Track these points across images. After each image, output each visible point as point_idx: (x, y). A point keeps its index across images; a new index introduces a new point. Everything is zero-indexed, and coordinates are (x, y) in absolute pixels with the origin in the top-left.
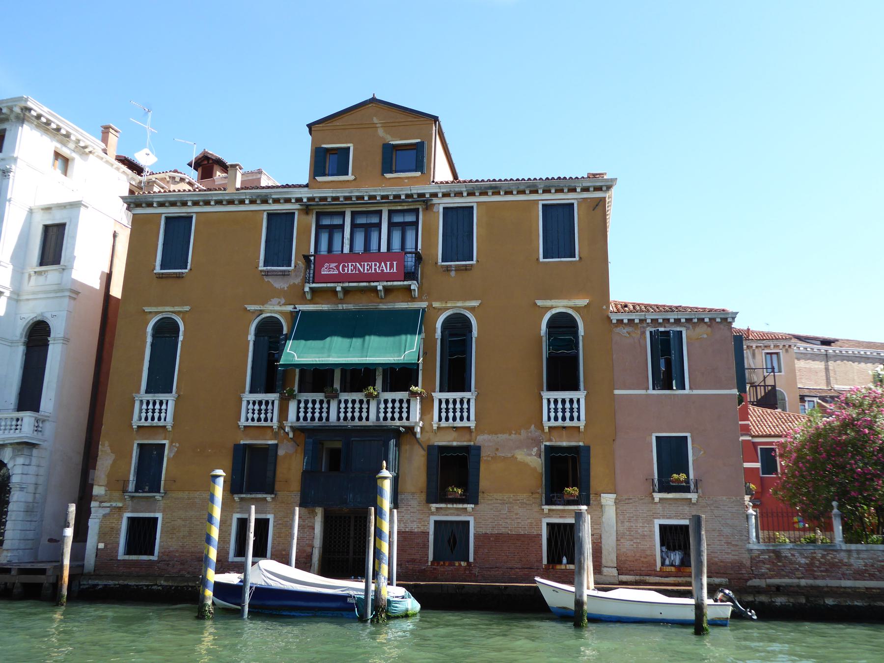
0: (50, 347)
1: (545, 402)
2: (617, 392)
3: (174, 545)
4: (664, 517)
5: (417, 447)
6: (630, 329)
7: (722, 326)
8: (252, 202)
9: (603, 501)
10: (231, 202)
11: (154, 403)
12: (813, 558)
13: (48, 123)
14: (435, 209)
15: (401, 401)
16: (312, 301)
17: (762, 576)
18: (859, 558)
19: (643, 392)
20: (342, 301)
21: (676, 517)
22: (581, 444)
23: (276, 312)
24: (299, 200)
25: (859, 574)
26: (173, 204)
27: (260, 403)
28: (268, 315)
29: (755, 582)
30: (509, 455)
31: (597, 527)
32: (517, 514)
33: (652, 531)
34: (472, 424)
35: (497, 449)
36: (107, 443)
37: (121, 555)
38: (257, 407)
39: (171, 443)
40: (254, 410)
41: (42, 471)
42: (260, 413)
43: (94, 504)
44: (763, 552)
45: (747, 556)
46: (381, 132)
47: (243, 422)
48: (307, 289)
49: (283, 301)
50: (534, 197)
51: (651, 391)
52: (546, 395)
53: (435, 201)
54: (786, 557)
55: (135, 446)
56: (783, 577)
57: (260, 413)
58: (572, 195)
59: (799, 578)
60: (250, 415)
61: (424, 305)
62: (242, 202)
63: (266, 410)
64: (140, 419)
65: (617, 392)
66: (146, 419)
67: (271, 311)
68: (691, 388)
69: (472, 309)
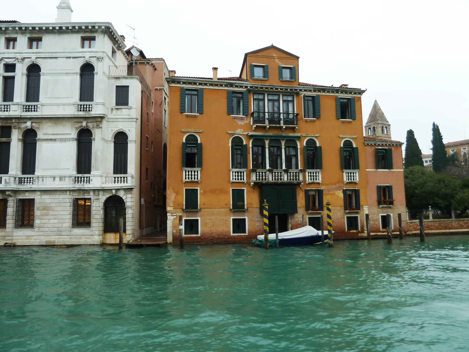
0: (129, 144)
2: (367, 170)
3: (207, 230)
5: (300, 190)
8: (226, 86)
9: (364, 209)
10: (216, 85)
11: (192, 172)
15: (296, 173)
16: (254, 131)
17: (411, 231)
20: (267, 131)
24: (246, 87)
26: (190, 83)
27: (238, 173)
33: (379, 218)
36: (171, 189)
37: (184, 235)
38: (237, 174)
42: (238, 177)
43: (168, 214)
46: (277, 61)
49: (242, 130)
52: (345, 171)
53: (301, 93)
57: (238, 177)
60: (234, 177)
61: (299, 135)
62: (221, 85)
63: (241, 175)
64: (186, 178)
65: (367, 170)
66: (189, 178)
67: (238, 134)
69: (317, 137)
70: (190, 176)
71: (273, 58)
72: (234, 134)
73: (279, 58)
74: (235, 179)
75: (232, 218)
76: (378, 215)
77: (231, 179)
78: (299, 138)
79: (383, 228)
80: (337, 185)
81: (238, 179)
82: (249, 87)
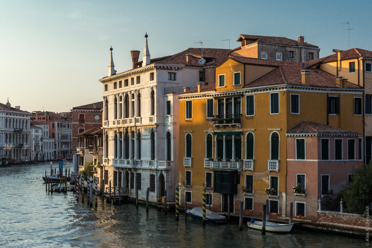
2: (288, 160)
6: (291, 138)
7: (315, 137)
12: (334, 216)
13: (164, 67)
14: (244, 97)
18: (346, 217)
19: (293, 160)
23: (210, 132)
24: (213, 95)
25: (346, 222)
28: (209, 133)
29: (318, 222)
30: (262, 179)
31: (281, 202)
34: (252, 169)
36: (180, 171)
39: (192, 171)
41: (172, 177)
44: (321, 213)
45: (317, 214)
47: (205, 166)
48: (214, 126)
50: (268, 91)
51: (296, 160)
54: (327, 215)
56: (325, 221)
58: (277, 91)
59: (329, 222)
65: (288, 160)
67: (210, 132)
68: (306, 159)
72: (208, 132)
79: (298, 215)
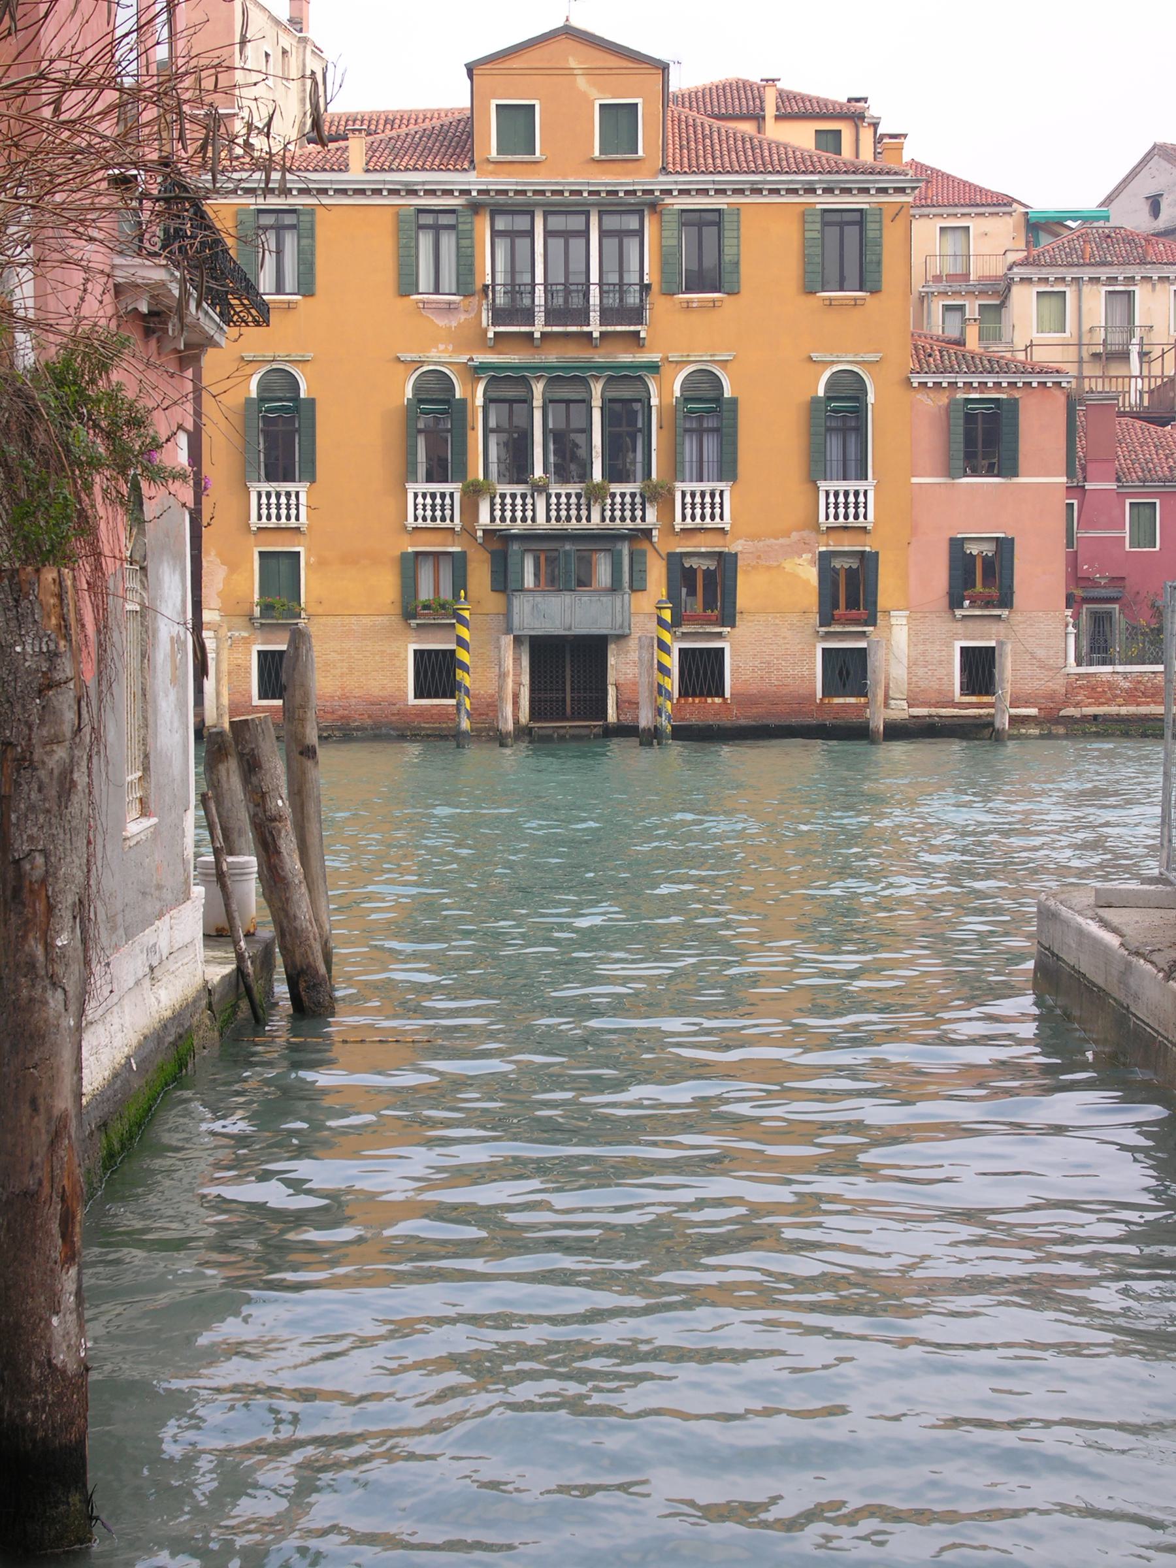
1: (822, 496)
2: (914, 480)
4: (966, 638)
9: (893, 621)
11: (278, 496)
16: (493, 349)
21: (982, 638)
22: (868, 549)
24: (463, 192)
32: (784, 638)
33: (951, 656)
35: (759, 557)
38: (429, 501)
40: (424, 505)
42: (433, 510)
46: (582, 83)
55: (256, 556)
57: (433, 510)
60: (420, 512)
64: (260, 518)
65: (914, 480)
66: (269, 518)
67: (436, 363)
70: (274, 511)
71: (569, 72)
73: (589, 72)
74: (424, 519)
75: (412, 647)
76: (950, 645)
77: (411, 518)
78: (654, 368)
80: (795, 536)
81: (434, 519)
82: (474, 194)
